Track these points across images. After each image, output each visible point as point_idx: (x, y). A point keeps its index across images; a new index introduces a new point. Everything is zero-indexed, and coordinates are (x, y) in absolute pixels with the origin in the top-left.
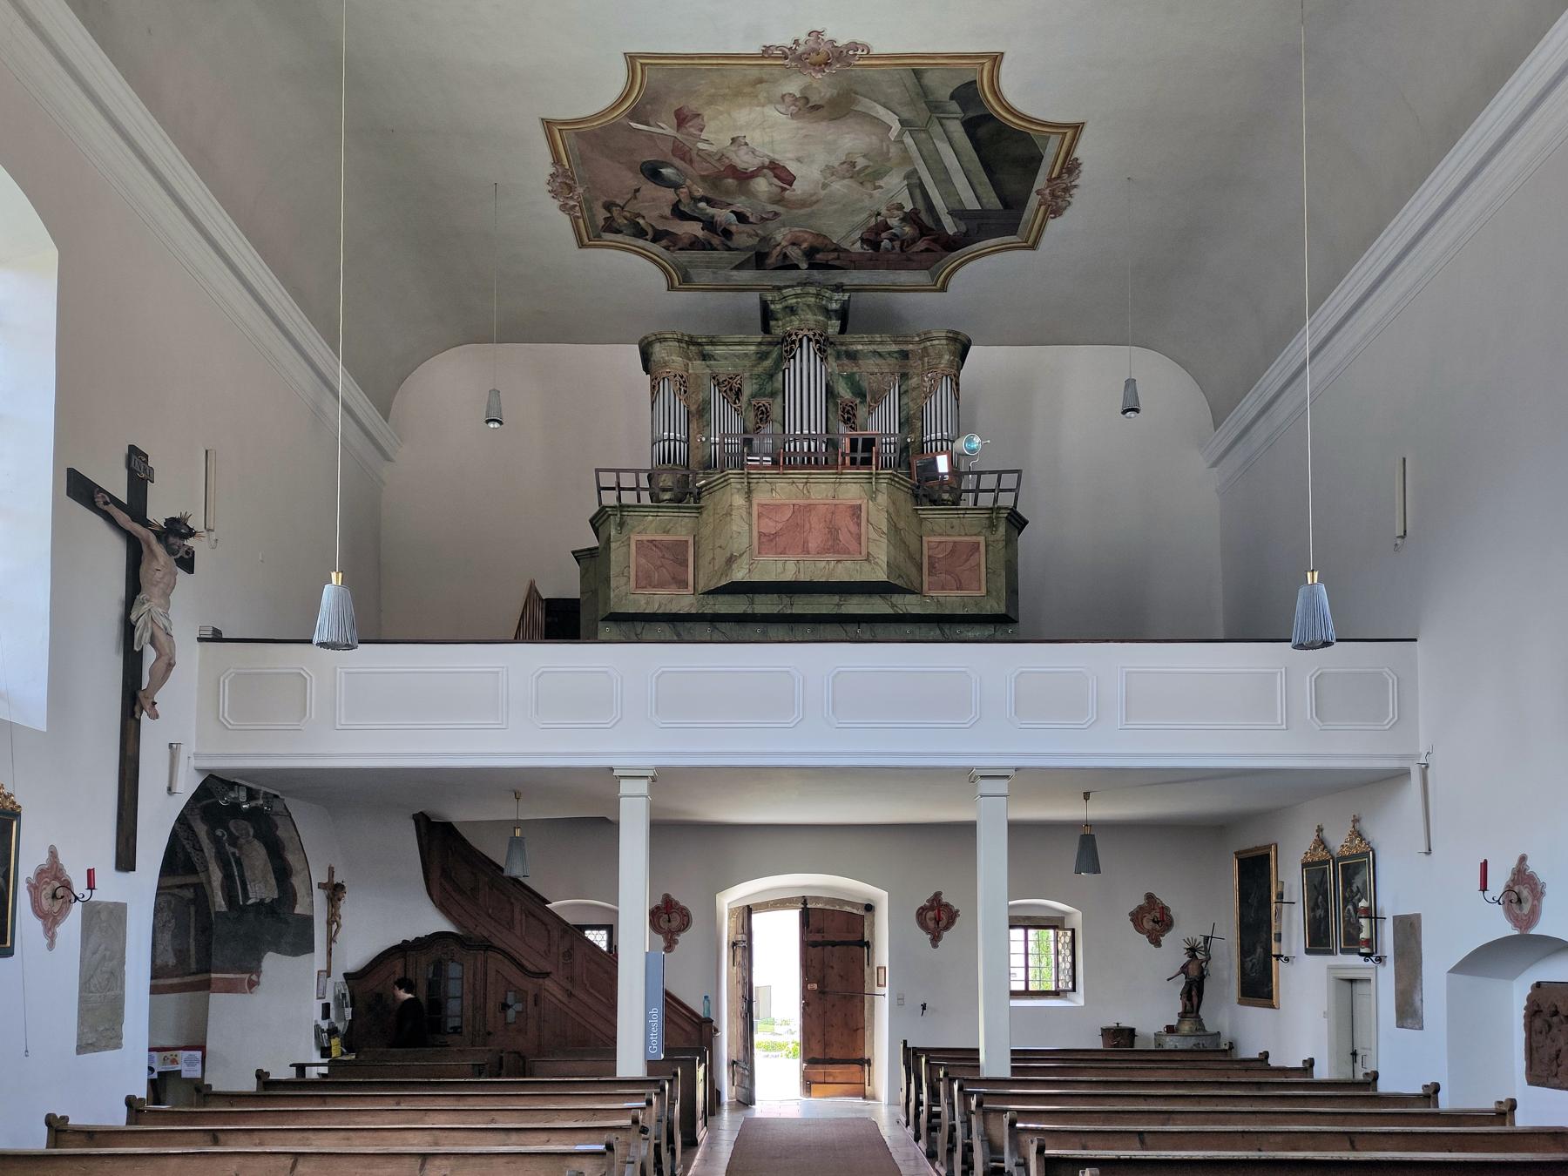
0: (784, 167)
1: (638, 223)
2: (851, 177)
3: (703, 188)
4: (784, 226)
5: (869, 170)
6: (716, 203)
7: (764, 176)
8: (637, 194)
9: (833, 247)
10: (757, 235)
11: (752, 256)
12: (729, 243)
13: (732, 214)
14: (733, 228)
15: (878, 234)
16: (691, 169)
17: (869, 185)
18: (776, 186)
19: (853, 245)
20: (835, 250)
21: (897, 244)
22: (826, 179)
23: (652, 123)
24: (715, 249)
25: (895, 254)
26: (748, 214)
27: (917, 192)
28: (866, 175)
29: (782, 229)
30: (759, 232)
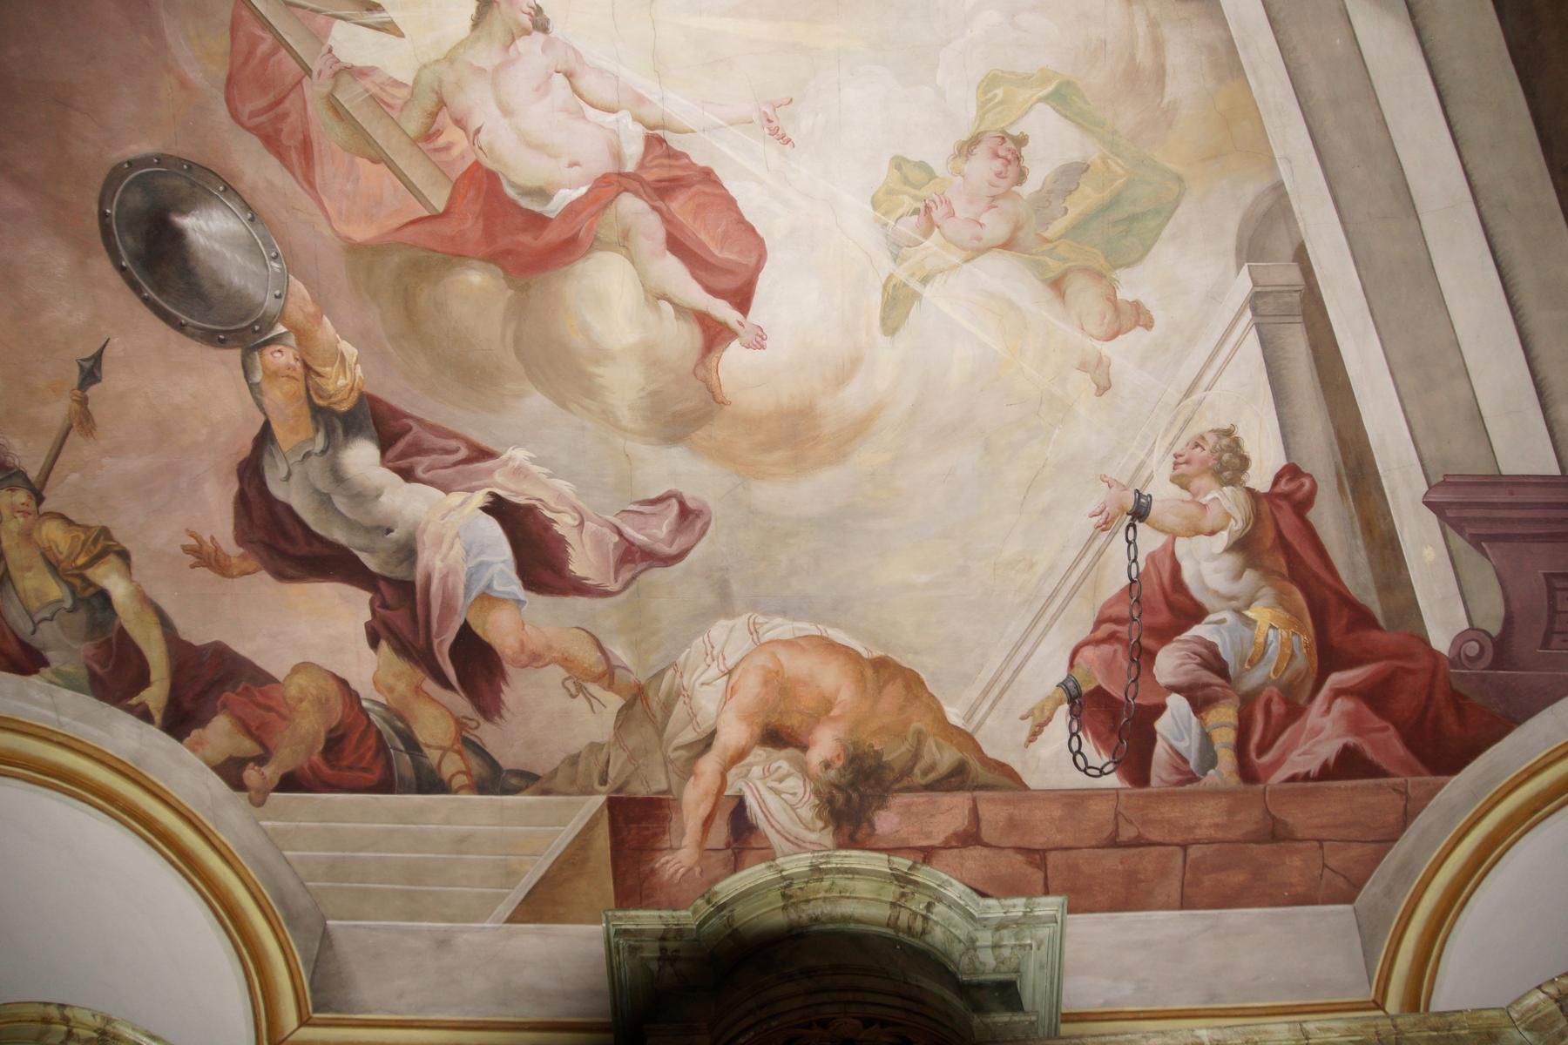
0: (708, 176)
1: (104, 597)
2: (1008, 245)
3: (362, 338)
4: (724, 605)
5: (1087, 197)
6: (418, 450)
7: (624, 243)
8: (93, 391)
9: (945, 757)
10: (608, 675)
11: (591, 826)
12: (488, 734)
13: (492, 529)
14: (500, 630)
15: (1143, 657)
16: (305, 201)
17: (1086, 295)
18: (680, 310)
19: (1034, 736)
20: (956, 779)
21: (1224, 717)
22: (895, 258)
24: (431, 783)
25: (1215, 793)
26: (564, 524)
27: (1296, 343)
28: (1077, 229)
29: (719, 630)
30: (620, 652)
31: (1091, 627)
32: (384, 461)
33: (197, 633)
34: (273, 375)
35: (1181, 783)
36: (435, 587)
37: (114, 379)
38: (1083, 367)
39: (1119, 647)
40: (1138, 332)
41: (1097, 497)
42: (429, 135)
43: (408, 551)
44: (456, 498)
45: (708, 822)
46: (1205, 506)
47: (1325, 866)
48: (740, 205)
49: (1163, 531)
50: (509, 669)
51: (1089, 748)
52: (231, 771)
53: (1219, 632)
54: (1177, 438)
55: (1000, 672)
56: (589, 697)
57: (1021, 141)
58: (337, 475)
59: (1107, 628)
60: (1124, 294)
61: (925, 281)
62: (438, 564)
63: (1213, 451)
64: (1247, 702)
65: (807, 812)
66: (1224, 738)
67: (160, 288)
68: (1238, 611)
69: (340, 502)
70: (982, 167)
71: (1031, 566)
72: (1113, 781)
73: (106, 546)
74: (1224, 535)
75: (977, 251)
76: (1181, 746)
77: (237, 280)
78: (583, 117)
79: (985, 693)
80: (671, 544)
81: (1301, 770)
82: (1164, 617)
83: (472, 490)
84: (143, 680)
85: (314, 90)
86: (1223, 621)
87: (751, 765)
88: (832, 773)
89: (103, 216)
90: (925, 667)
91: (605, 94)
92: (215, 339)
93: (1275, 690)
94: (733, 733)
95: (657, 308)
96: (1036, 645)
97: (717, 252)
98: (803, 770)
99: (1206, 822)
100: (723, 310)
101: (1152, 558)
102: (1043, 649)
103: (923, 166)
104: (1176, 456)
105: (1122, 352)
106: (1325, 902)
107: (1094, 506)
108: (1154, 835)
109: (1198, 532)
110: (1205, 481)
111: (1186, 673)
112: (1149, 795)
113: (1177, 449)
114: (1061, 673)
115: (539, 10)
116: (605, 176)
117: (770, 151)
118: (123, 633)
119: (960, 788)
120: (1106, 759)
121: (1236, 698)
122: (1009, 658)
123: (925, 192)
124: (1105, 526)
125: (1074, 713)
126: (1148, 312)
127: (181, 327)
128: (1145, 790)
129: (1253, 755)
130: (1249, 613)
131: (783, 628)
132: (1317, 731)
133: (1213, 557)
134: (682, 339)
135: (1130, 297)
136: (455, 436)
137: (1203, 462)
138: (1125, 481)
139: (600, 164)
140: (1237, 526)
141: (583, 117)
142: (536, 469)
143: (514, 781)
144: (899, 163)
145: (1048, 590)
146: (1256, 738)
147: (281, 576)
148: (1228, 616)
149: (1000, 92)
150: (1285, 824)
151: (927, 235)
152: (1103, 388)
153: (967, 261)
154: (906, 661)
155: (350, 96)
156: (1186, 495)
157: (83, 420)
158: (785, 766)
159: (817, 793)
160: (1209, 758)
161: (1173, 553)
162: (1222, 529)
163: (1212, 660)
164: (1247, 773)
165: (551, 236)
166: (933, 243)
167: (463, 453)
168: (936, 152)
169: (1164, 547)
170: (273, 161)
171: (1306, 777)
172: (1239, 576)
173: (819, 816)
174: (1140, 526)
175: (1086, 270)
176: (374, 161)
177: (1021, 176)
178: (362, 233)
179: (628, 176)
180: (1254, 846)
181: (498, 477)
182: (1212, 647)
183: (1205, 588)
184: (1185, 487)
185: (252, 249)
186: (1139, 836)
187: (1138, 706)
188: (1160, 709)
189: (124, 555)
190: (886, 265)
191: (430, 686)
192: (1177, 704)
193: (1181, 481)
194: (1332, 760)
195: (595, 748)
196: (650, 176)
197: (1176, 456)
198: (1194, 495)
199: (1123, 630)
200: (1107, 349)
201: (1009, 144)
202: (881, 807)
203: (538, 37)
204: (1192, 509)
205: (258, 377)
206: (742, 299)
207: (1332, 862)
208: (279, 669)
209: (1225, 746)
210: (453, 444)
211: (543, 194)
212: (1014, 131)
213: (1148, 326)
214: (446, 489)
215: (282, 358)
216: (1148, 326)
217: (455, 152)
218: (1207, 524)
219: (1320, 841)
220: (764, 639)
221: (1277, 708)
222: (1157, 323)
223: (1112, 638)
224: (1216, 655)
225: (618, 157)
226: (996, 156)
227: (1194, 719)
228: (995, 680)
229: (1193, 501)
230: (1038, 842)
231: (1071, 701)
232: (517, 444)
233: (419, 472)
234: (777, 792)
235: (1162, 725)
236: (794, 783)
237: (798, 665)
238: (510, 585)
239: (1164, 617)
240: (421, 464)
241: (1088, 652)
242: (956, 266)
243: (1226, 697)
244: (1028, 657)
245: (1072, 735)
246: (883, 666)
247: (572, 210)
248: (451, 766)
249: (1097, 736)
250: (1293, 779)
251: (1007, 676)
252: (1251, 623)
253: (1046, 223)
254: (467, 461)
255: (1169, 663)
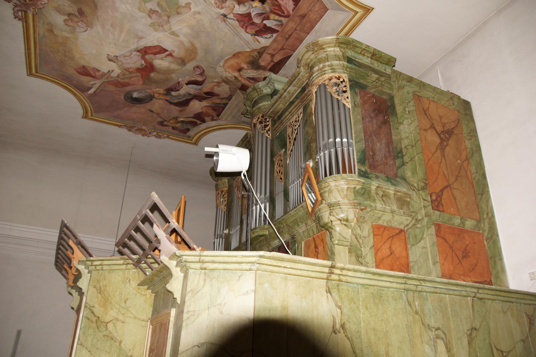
2: (169, 17)
9: (256, 54)
13: (190, 86)
15: (253, 24)
19: (259, 42)
21: (272, 16)
22: (166, 31)
23: (90, 86)
24: (226, 104)
31: (243, 29)
32: (175, 92)
33: (192, 115)
34: (158, 97)
35: (282, 26)
36: (196, 93)
37: (153, 110)
38: (194, 15)
39: (249, 26)
40: (191, 5)
41: (219, 21)
42: (129, 72)
43: (190, 94)
44: (184, 87)
45: (249, 82)
46: (228, 6)
47: (316, 11)
48: (151, 45)
49: (230, 14)
50: (213, 91)
51: (266, 36)
52: (213, 120)
53: (255, 12)
54: (214, 6)
55: (244, 42)
56: (221, 86)
57: (151, 9)
58: (174, 96)
59: (244, 27)
60: (183, 5)
61: (171, 29)
62: (193, 92)
63: (219, 2)
64: (272, 12)
65: (255, 72)
66: (277, 17)
67: (142, 102)
68: (252, 8)
69: (179, 97)
70: (154, 16)
71: (227, 33)
72: (275, 35)
73: (176, 118)
74: (235, 5)
75: (168, 22)
76: (274, 24)
77: (144, 95)
78: (131, 57)
79: (247, 45)
80: (201, 70)
81: (292, 8)
82: (247, 19)
83: (183, 85)
84: (196, 122)
85: (119, 80)
86: (253, 11)
87: (243, 74)
88: (250, 66)
89: (131, 103)
90: (238, 50)
91: (129, 54)
92: (151, 100)
93: (272, 7)
94: (236, 74)
95: (164, 59)
96: (242, 37)
97: (156, 51)
98: (246, 69)
99: (293, 25)
100: (167, 53)
101: (234, 17)
102: (244, 36)
103: (152, 23)
104: (217, 7)
105: (193, 8)
106: (325, 14)
107: (220, 22)
108: (290, 33)
109: (233, 9)
110: (224, 5)
111: (260, 19)
112: (281, 31)
113: (216, 7)
114: (250, 36)
115: (114, 56)
116: (142, 58)
117: (143, 40)
118: (188, 121)
119: (262, 54)
120: (270, 35)
121: (270, 13)
122: (243, 41)
123: (156, 25)
124: (225, 21)
125: (258, 36)
126: (188, 3)
127: (148, 102)
128: (280, 32)
129: (284, 15)
130: (254, 6)
131: (222, 64)
132: (286, 3)
133: (239, 8)
134: (170, 58)
135: (184, 4)
136: (175, 84)
137: (220, 4)
138: (218, 16)
139: (140, 58)
140: (235, 3)
141: (131, 57)
142: (183, 79)
143: (230, 97)
144: (150, 26)
145: (233, 32)
146: (280, 13)
147: (188, 105)
148: (252, 10)
149: (142, 9)
150: (302, 14)
151: (163, 27)
152: (199, 13)
153: (169, 23)
154: (235, 52)
155: (122, 77)
156: (225, 8)
157: (158, 114)
158: (245, 71)
159: (252, 69)
160: (281, 21)
161: (236, 14)
162: (234, 5)
163: (260, 15)
164: (288, 16)
165: (149, 66)
166: (165, 27)
167: (178, 85)
168: (149, 21)
169: (233, 15)
170: (128, 87)
171: (294, 8)
172: (245, 6)
173: (256, 70)
174: (227, 16)
175: (177, 9)
176: (131, 78)
177: (158, 12)
178: (141, 82)
179: (142, 56)
180: (303, 20)
181: (183, 82)
182: (257, 14)
183: (244, 11)
184: (223, 8)
185: (140, 93)
186: (289, 35)
187: (262, 27)
188: (265, 25)
189: (177, 117)
190: (166, 33)
191: (211, 99)
192: (265, 22)
193: (222, 8)
194: (294, 3)
195: (229, 88)
196: (143, 53)
197: (217, 7)
198: (226, 7)
199: (246, 25)
200: (192, 10)
201: (151, 11)
202: (260, 63)
203: (118, 57)
204: (228, 8)
205: (158, 98)
206: (166, 51)
207: (316, 10)
208: (201, 111)
209: (279, 18)
210: (176, 85)
211: (142, 65)
212: (149, 10)
213: (190, 3)
214: (182, 88)
215: (156, 95)
216: (190, 3)
217: (133, 70)
218: (232, 7)
219: (310, 10)
220: (222, 66)
221: (276, 8)
222: (190, 2)
223: (247, 27)
224: (260, 13)
225: (139, 56)
226: (153, 14)
227: (270, 20)
228: (245, 43)
229: (227, 8)
230: (280, 48)
231: (255, 35)
232: (179, 79)
233: (178, 89)
234: (249, 73)
235: (268, 25)
236: (249, 71)
237: (229, 63)
238: (200, 87)
239: (247, 19)
240: (177, 88)
241: (247, 30)
242: (170, 25)
243: (269, 15)
244: (244, 38)
245: (262, 37)
246: (234, 55)
247: (145, 62)
248: (224, 101)
249: (265, 34)
250: (293, 10)
251: (245, 42)
252: (256, 7)
253: (167, 11)
254: (179, 84)
255: (257, 21)
